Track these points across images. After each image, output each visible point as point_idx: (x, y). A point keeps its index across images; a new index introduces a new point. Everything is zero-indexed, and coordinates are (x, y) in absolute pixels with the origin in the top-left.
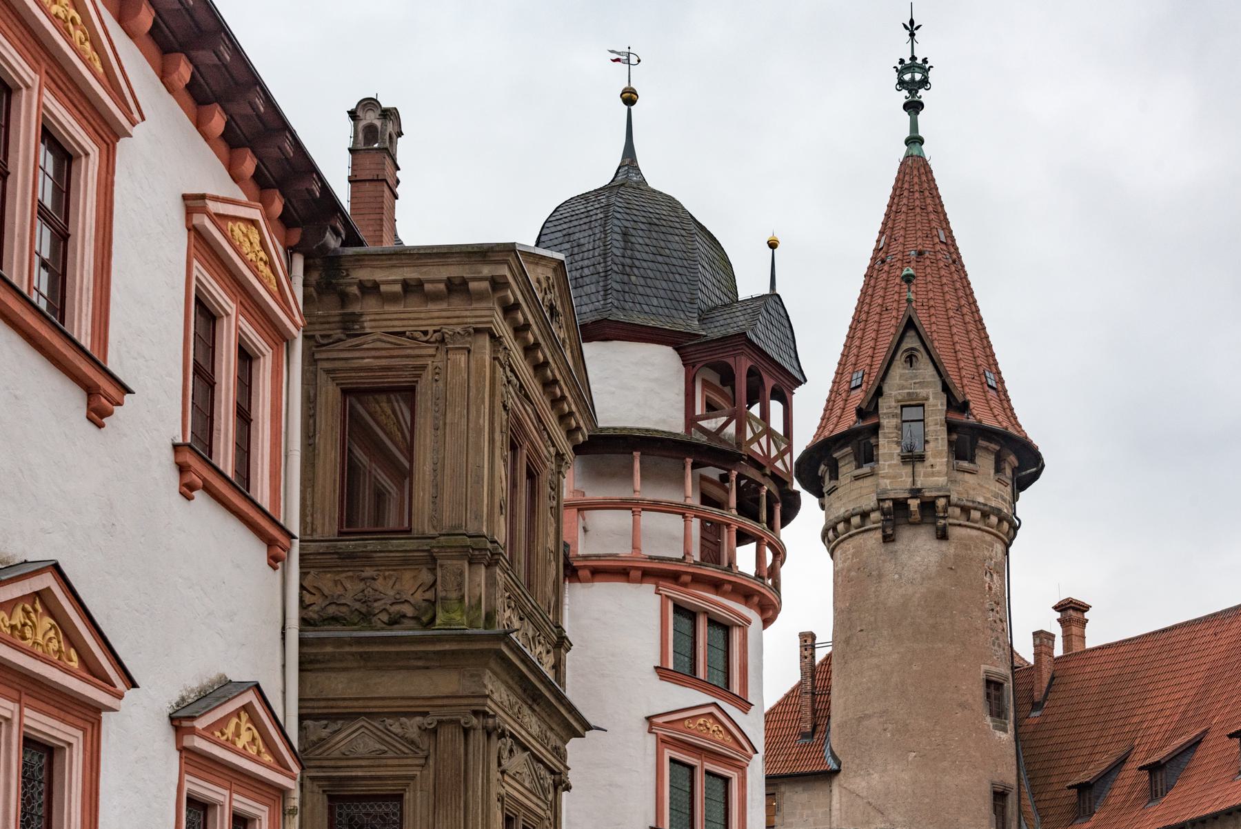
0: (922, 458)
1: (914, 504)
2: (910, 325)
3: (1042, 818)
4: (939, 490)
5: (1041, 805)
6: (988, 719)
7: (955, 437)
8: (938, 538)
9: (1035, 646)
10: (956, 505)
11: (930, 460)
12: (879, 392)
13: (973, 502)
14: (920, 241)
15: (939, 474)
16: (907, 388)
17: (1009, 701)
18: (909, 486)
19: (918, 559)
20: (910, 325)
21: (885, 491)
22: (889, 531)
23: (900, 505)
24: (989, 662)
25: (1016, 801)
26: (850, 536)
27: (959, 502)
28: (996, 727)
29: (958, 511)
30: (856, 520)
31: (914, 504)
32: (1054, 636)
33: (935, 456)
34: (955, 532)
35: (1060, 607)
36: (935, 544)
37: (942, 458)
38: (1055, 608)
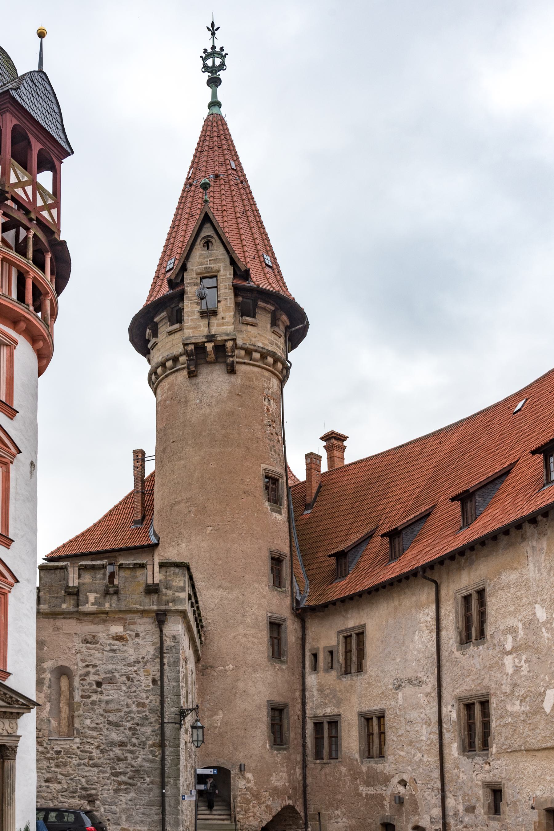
0: (215, 313)
1: (209, 346)
2: (206, 219)
3: (311, 581)
4: (228, 335)
5: (311, 572)
6: (267, 503)
7: (240, 299)
8: (228, 373)
9: (307, 464)
10: (241, 348)
11: (221, 314)
12: (184, 268)
13: (254, 346)
14: (217, 168)
15: (227, 324)
16: (204, 264)
17: (283, 493)
18: (206, 333)
19: (214, 388)
20: (206, 219)
21: (188, 338)
22: (193, 368)
23: (200, 348)
24: (267, 462)
25: (289, 566)
26: (166, 376)
27: (244, 346)
28: (272, 510)
29: (243, 353)
30: (169, 364)
31: (209, 346)
32: (321, 457)
33: (224, 311)
34: (241, 369)
35: (327, 438)
36: (226, 377)
37: (230, 312)
38: (322, 438)
